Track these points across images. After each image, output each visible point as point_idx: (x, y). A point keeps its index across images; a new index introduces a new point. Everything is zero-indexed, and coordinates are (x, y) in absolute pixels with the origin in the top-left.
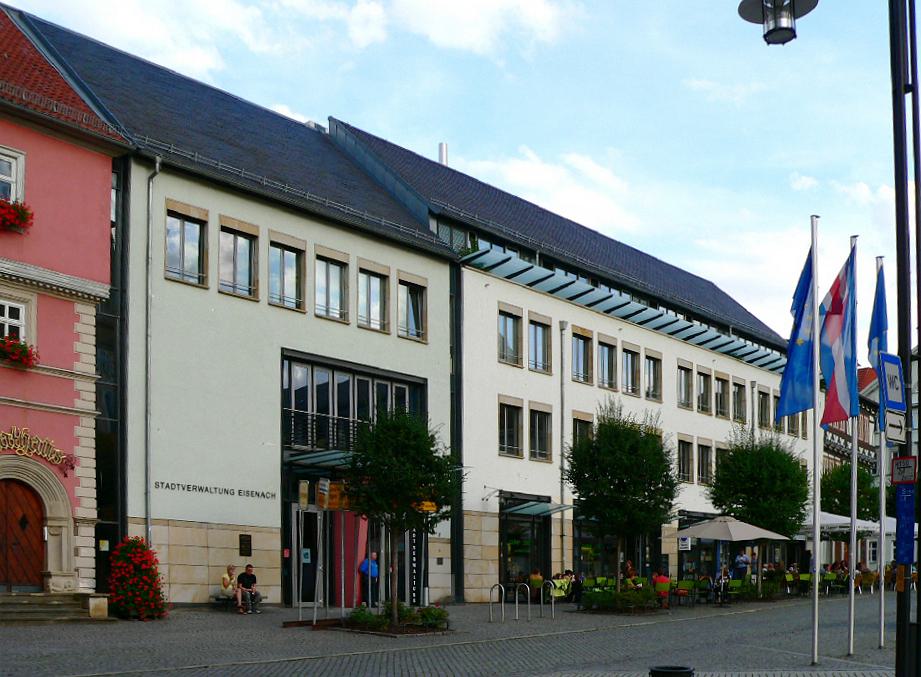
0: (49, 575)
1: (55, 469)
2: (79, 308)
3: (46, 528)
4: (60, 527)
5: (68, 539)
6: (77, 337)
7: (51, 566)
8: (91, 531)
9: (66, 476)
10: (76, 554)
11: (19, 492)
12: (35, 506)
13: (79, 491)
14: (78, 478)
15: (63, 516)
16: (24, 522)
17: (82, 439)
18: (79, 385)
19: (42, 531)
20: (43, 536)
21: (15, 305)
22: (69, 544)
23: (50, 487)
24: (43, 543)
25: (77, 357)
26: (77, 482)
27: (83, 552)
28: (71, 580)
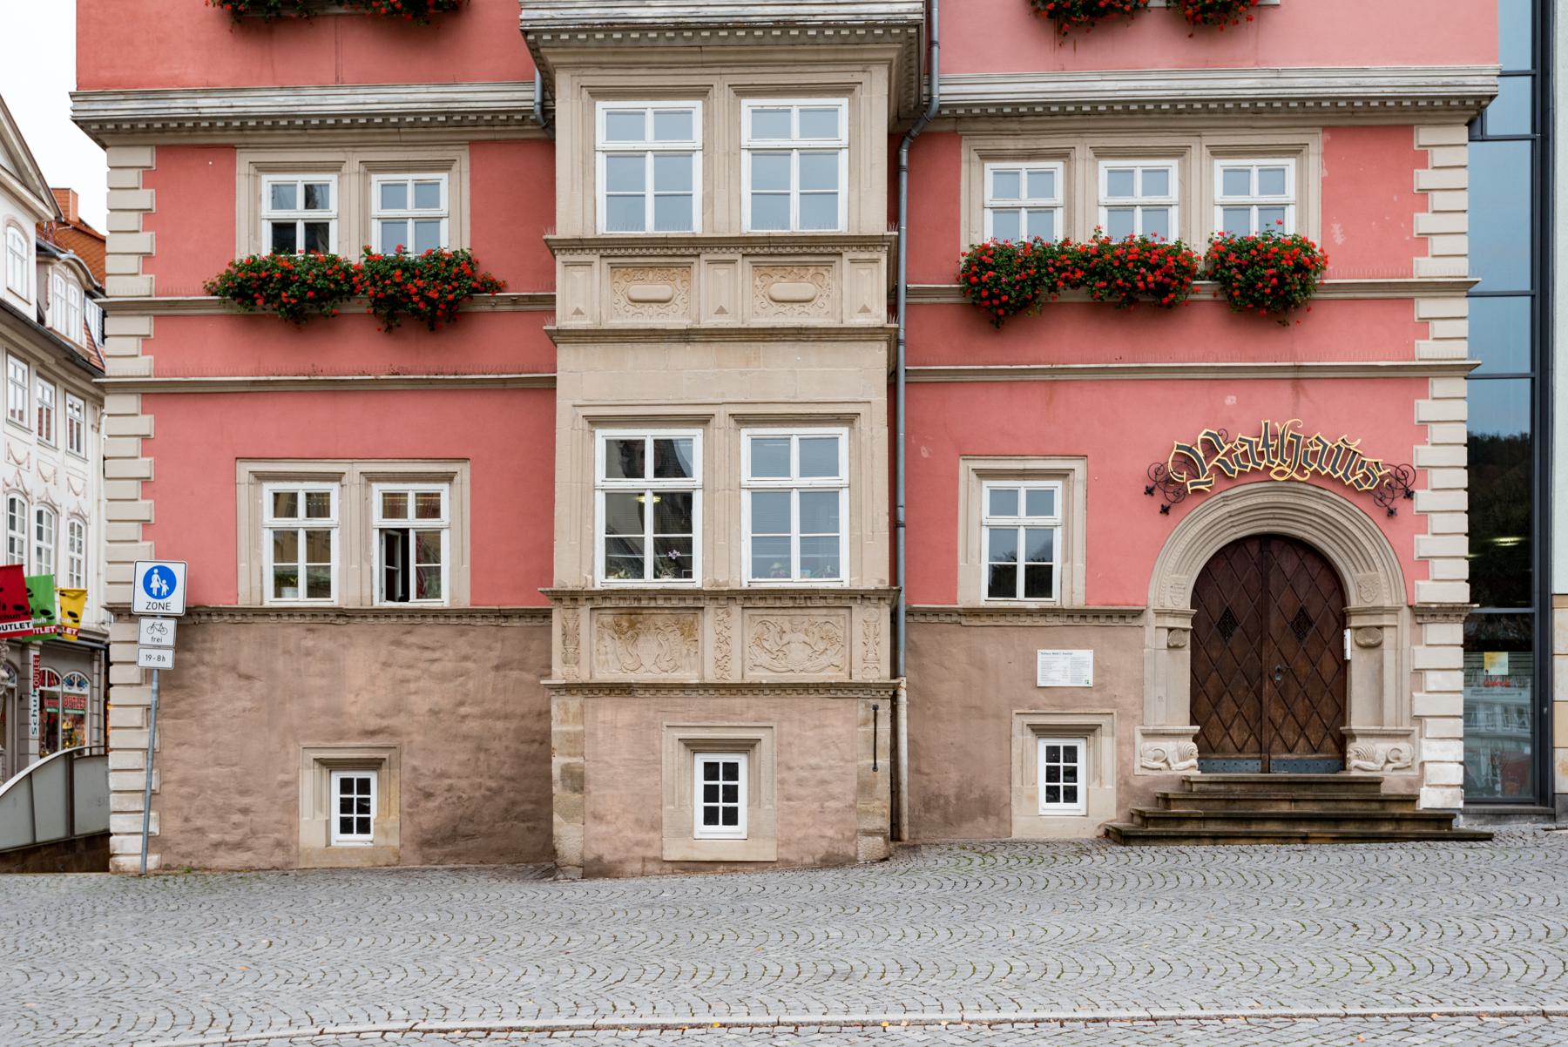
0: (1353, 737)
3: (1348, 633)
4: (1380, 628)
5: (1397, 649)
7: (1359, 717)
11: (1288, 562)
12: (1326, 585)
15: (1387, 603)
16: (1301, 623)
19: (1342, 638)
20: (1343, 651)
22: (1399, 663)
24: (1344, 665)
28: (1403, 745)
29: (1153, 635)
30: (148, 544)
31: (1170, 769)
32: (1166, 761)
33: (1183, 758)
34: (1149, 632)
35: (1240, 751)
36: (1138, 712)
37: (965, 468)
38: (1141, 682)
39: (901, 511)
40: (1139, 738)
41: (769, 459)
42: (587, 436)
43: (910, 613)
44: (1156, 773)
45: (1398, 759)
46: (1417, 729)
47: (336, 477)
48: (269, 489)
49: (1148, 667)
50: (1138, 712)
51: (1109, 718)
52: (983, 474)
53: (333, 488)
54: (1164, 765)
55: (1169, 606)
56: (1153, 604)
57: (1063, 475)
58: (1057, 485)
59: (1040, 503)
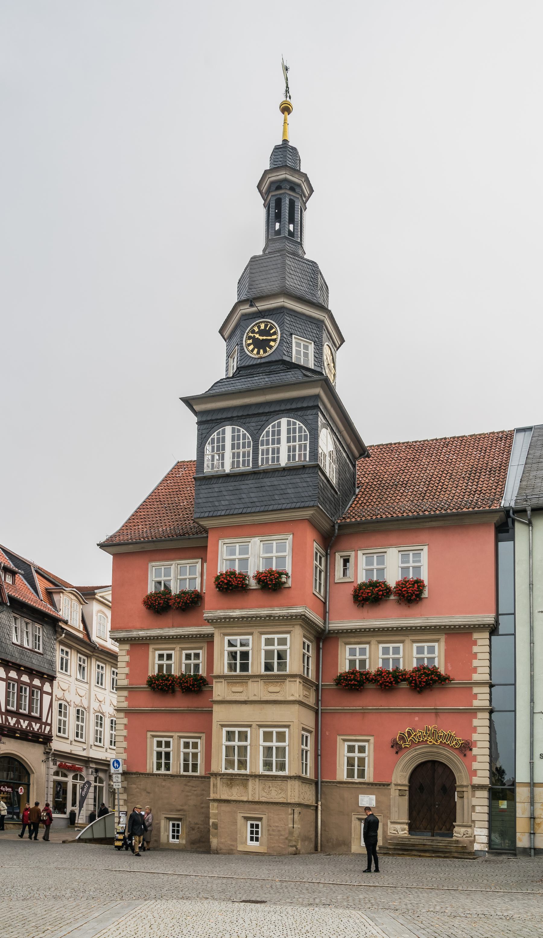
1: (457, 751)
2: (476, 636)
3: (456, 792)
6: (475, 656)
8: (485, 794)
9: (465, 755)
10: (474, 810)
13: (475, 766)
14: (475, 756)
17: (478, 728)
18: (476, 690)
21: (169, 652)
23: (455, 763)
25: (475, 670)
26: (474, 758)
27: (478, 809)
29: (394, 792)
30: (125, 754)
31: (398, 834)
32: (397, 831)
33: (402, 831)
34: (392, 791)
35: (425, 829)
36: (389, 815)
37: (339, 738)
38: (390, 806)
39: (319, 751)
40: (389, 823)
41: (268, 736)
42: (220, 729)
43: (322, 782)
44: (394, 835)
45: (467, 834)
46: (473, 824)
47: (171, 737)
48: (155, 739)
49: (392, 801)
50: (389, 815)
51: (380, 817)
52: (345, 740)
53: (171, 740)
54: (396, 832)
55: (399, 782)
56: (394, 782)
57: (368, 741)
58: (366, 744)
59: (362, 749)
